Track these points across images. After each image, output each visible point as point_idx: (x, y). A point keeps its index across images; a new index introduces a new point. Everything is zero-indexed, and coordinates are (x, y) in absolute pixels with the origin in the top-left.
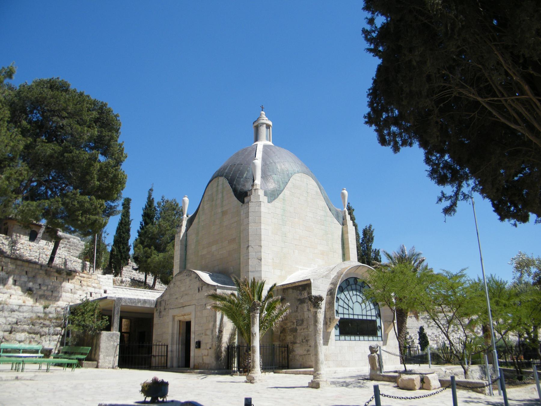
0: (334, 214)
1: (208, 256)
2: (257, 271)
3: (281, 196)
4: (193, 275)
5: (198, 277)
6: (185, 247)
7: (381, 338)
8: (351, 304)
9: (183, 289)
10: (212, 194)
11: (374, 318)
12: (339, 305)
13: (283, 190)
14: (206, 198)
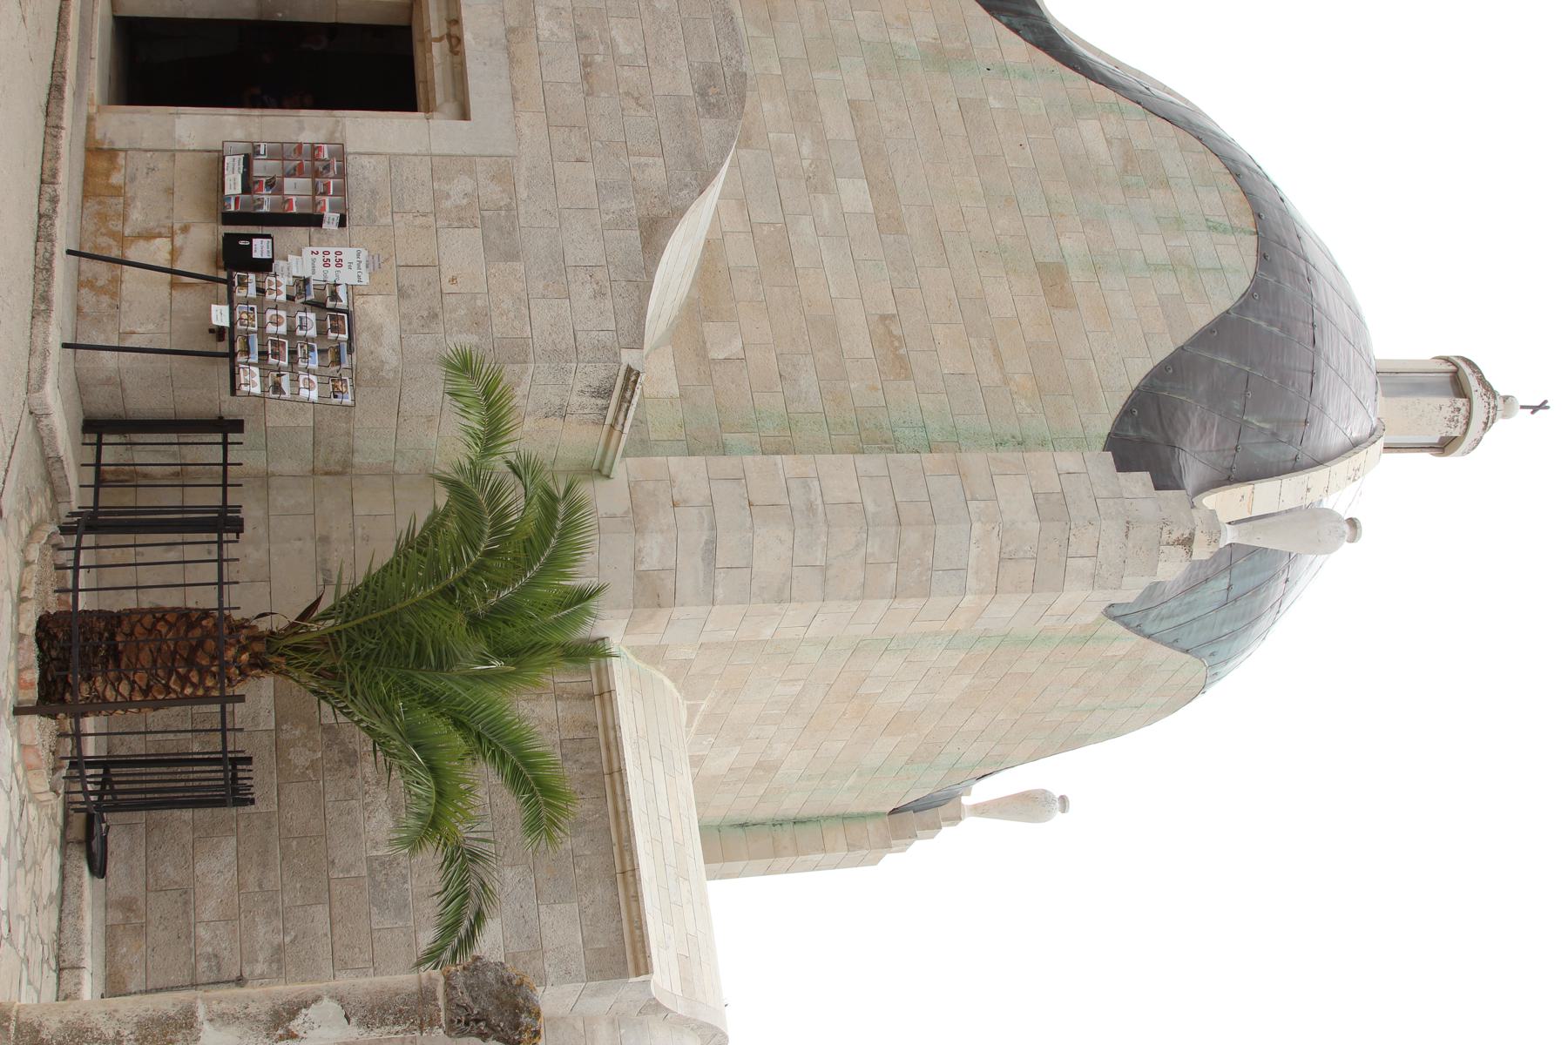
1: (805, 151)
9: (618, 33)
10: (1165, 183)
14: (1143, 131)
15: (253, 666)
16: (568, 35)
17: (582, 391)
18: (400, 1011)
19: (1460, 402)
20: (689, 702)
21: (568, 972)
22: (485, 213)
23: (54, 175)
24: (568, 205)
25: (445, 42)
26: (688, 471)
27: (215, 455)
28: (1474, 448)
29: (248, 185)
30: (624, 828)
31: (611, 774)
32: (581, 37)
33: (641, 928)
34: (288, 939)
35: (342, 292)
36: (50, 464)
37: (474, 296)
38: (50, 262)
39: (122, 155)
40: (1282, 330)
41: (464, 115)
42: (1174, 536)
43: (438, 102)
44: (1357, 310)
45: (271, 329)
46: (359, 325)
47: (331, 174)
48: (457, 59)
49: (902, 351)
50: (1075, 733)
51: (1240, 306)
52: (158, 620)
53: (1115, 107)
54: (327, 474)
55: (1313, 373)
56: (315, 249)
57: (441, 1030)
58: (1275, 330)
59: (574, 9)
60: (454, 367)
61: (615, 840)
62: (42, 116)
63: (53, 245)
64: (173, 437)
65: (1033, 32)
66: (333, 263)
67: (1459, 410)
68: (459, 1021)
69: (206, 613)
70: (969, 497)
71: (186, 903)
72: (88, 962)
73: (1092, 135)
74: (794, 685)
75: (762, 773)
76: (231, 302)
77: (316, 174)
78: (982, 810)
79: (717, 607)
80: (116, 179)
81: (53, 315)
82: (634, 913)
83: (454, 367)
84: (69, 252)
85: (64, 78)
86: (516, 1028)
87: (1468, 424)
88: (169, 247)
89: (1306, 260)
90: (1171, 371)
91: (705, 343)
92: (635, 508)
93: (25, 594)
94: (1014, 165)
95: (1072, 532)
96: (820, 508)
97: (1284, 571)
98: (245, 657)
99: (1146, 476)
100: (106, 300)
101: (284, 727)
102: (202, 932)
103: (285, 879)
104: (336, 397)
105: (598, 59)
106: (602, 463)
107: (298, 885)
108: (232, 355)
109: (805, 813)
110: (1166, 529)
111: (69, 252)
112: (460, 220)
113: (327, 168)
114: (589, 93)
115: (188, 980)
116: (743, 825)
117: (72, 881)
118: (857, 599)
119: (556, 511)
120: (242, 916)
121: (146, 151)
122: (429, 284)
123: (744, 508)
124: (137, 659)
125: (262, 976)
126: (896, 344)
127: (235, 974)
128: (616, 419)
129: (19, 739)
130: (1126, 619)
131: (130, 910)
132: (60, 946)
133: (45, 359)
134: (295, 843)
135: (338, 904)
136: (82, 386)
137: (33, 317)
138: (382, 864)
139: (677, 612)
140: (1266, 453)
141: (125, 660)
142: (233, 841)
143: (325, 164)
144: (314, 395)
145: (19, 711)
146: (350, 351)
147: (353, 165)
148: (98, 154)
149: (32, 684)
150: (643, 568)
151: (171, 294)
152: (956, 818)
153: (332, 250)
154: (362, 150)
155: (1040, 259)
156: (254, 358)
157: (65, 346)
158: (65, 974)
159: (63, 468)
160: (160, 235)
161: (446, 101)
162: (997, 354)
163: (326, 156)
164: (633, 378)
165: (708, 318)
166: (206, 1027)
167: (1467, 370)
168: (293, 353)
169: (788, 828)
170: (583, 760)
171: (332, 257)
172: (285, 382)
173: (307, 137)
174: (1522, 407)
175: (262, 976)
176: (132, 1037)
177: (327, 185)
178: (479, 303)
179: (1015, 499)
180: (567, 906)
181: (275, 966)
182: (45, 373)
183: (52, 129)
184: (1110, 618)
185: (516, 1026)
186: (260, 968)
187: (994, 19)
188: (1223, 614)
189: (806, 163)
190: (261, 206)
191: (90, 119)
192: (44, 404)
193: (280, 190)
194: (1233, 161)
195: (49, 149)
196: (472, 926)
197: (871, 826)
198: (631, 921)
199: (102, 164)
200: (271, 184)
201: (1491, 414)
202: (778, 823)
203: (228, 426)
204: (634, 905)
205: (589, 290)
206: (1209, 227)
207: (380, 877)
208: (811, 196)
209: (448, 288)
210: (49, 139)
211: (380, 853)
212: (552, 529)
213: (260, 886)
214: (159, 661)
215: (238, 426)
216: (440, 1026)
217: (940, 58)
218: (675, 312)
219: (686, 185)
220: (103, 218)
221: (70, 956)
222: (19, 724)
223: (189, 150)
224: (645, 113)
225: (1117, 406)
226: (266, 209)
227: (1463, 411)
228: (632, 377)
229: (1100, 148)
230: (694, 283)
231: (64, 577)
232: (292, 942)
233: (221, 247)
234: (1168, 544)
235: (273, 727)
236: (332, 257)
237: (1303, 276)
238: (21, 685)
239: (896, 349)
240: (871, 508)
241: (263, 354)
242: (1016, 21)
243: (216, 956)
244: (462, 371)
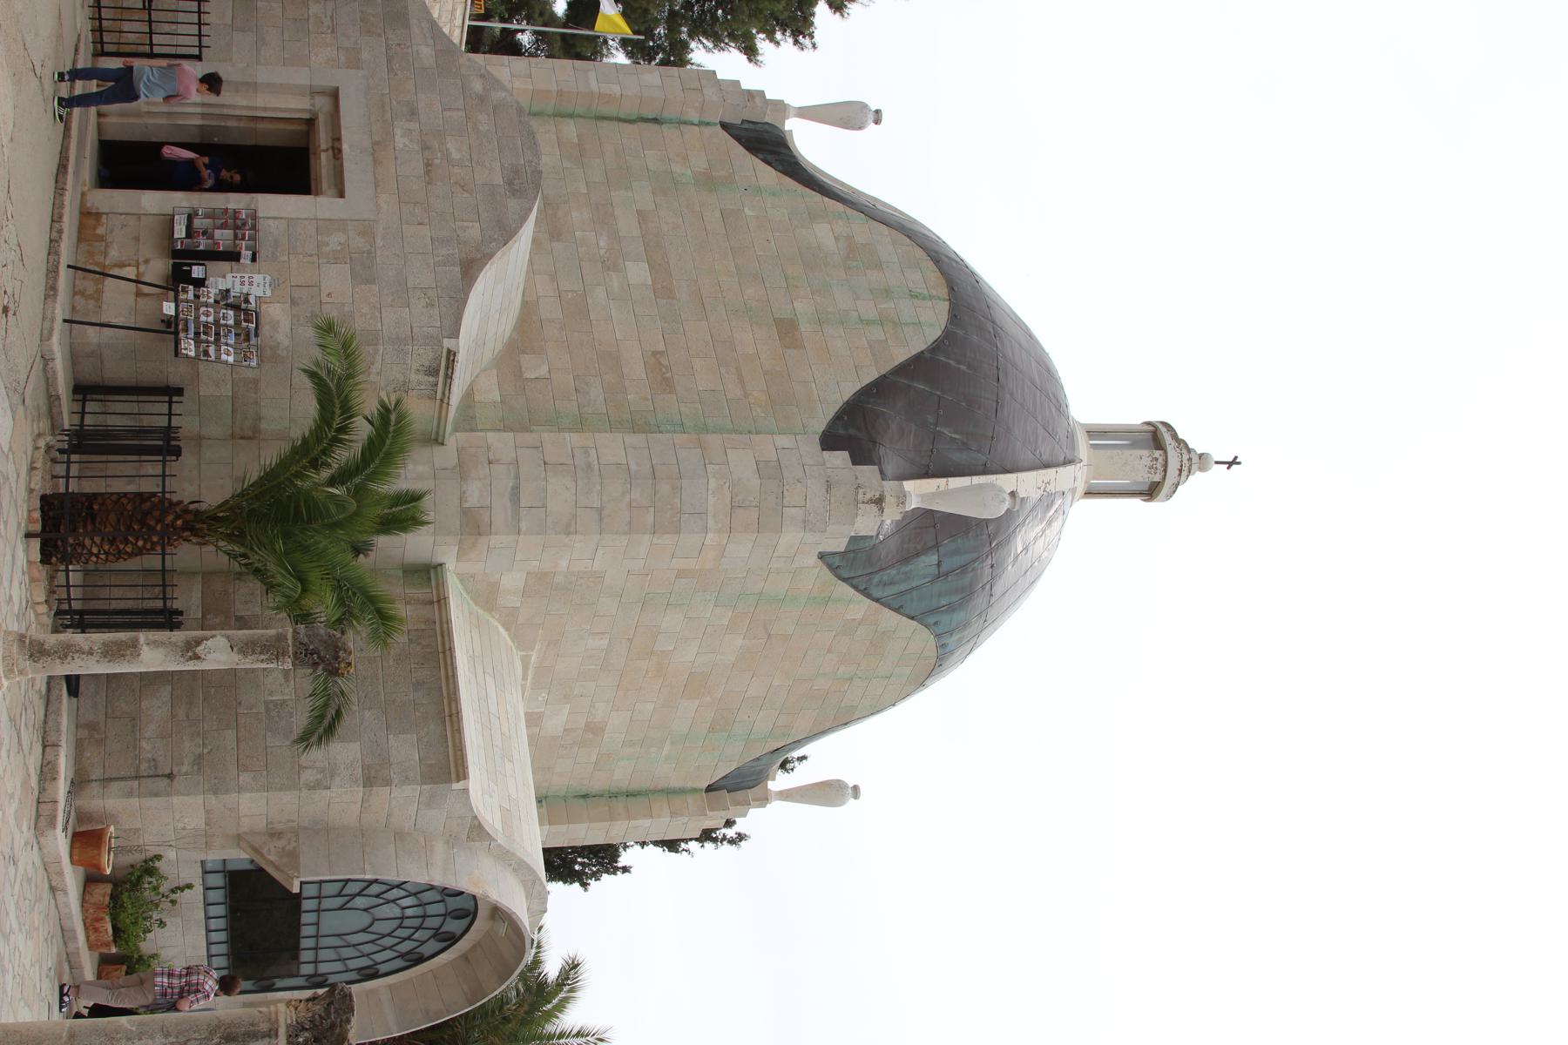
0: (755, 764)
1: (602, 244)
2: (516, 516)
3: (845, 590)
4: (513, 204)
5: (507, 234)
6: (650, 117)
8: (360, 902)
10: (879, 266)
11: (307, 969)
13: (869, 596)
14: (861, 229)
15: (184, 529)
16: (416, 147)
17: (418, 370)
18: (265, 645)
19: (1157, 453)
20: (522, 653)
21: (407, 778)
22: (353, 255)
23: (61, 217)
24: (411, 251)
25: (330, 152)
26: (501, 443)
27: (164, 408)
28: (1174, 492)
29: (190, 232)
30: (451, 686)
31: (444, 652)
32: (425, 147)
33: (461, 750)
34: (206, 751)
35: (252, 299)
36: (52, 399)
37: (343, 304)
38: (57, 268)
39: (104, 216)
40: (969, 367)
41: (341, 195)
42: (868, 497)
43: (324, 189)
44: (1046, 365)
45: (203, 318)
46: (263, 321)
47: (247, 227)
48: (337, 162)
49: (669, 375)
50: (842, 704)
51: (933, 348)
52: (122, 497)
53: (843, 215)
54: (243, 438)
55: (997, 402)
56: (235, 275)
57: (289, 660)
58: (963, 367)
59: (421, 130)
60: (321, 329)
61: (445, 694)
62: (53, 182)
63: (59, 258)
64: (134, 398)
65: (783, 165)
66: (247, 283)
67: (1157, 459)
68: (301, 653)
69: (154, 494)
70: (707, 462)
71: (134, 726)
72: (63, 743)
73: (825, 234)
74: (602, 639)
75: (591, 736)
76: (176, 301)
77: (236, 228)
78: (787, 795)
79: (522, 536)
80: (100, 231)
81: (58, 297)
82: (457, 741)
83: (321, 329)
84: (69, 266)
85: (68, 160)
86: (336, 660)
87: (1165, 471)
88: (136, 272)
89: (994, 322)
90: (875, 391)
91: (521, 368)
92: (460, 464)
93: (35, 465)
94: (762, 253)
95: (786, 487)
96: (596, 467)
97: (987, 556)
98: (179, 522)
99: (846, 454)
100: (92, 303)
101: (208, 617)
102: (144, 744)
103: (205, 712)
104: (245, 361)
105: (437, 161)
106: (437, 433)
107: (215, 717)
108: (176, 333)
109: (635, 786)
110: (861, 491)
111: (69, 266)
112: (336, 259)
113: (244, 224)
114: (430, 182)
115: (133, 774)
116: (585, 796)
117: (55, 692)
118: (625, 533)
119: (389, 420)
120: (174, 736)
121: (121, 214)
122: (313, 297)
123: (540, 466)
124: (107, 519)
125: (186, 774)
126: (664, 370)
127: (167, 771)
128: (444, 393)
129: (27, 557)
130: (855, 582)
131: (94, 729)
132: (45, 732)
133: (53, 322)
134: (213, 690)
135: (243, 730)
136: (74, 357)
137: (45, 299)
138: (276, 705)
139: (494, 540)
140: (958, 457)
141: (98, 520)
142: (169, 688)
143: (243, 222)
144: (231, 359)
145: (28, 535)
146: (256, 335)
147: (261, 225)
148: (89, 217)
149: (37, 520)
150: (467, 505)
151: (136, 300)
152: (764, 800)
153: (247, 276)
154: (269, 215)
155: (776, 316)
156: (192, 336)
157: (65, 321)
158: (48, 749)
159: (60, 405)
160: (129, 265)
161: (329, 188)
162: (741, 380)
163: (244, 217)
164: (452, 358)
165: (524, 352)
166: (145, 647)
167: (1163, 429)
168: (217, 334)
169: (622, 799)
170: (424, 643)
171: (246, 279)
172: (212, 351)
173: (231, 206)
174: (1217, 463)
175: (186, 774)
176: (99, 651)
177: (244, 235)
178: (346, 309)
179: (742, 465)
180: (409, 736)
181: (196, 768)
182: (53, 330)
183: (59, 190)
184: (839, 579)
185: (336, 658)
186: (184, 769)
187: (753, 156)
188: (938, 587)
189: (602, 252)
190: (199, 246)
191: (83, 194)
192: (51, 351)
193: (212, 237)
194: (936, 252)
195: (57, 202)
196: (333, 719)
197: (690, 798)
198: (454, 746)
199: (92, 222)
200: (205, 233)
201: (1185, 461)
202: (614, 795)
203: (172, 392)
204: (457, 735)
205: (423, 302)
206: (912, 296)
207: (274, 714)
208: (605, 273)
209: (325, 299)
210: (57, 196)
211: (274, 698)
212: (387, 432)
213: (188, 717)
214: (122, 521)
215: (179, 391)
216: (289, 657)
217: (708, 181)
218: (499, 347)
219: (495, 240)
220: (91, 254)
221: (52, 738)
222: (28, 546)
223: (150, 214)
224: (468, 195)
225: (831, 412)
226: (201, 248)
227: (1160, 460)
228: (451, 356)
229: (830, 243)
230: (515, 328)
231: (57, 485)
232: (208, 752)
233: (170, 272)
234: (863, 502)
235: (200, 616)
236: (246, 279)
237: (989, 332)
238: (30, 520)
239: (664, 373)
240: (633, 467)
241: (197, 334)
242: (769, 157)
243: (154, 760)
244: (328, 332)
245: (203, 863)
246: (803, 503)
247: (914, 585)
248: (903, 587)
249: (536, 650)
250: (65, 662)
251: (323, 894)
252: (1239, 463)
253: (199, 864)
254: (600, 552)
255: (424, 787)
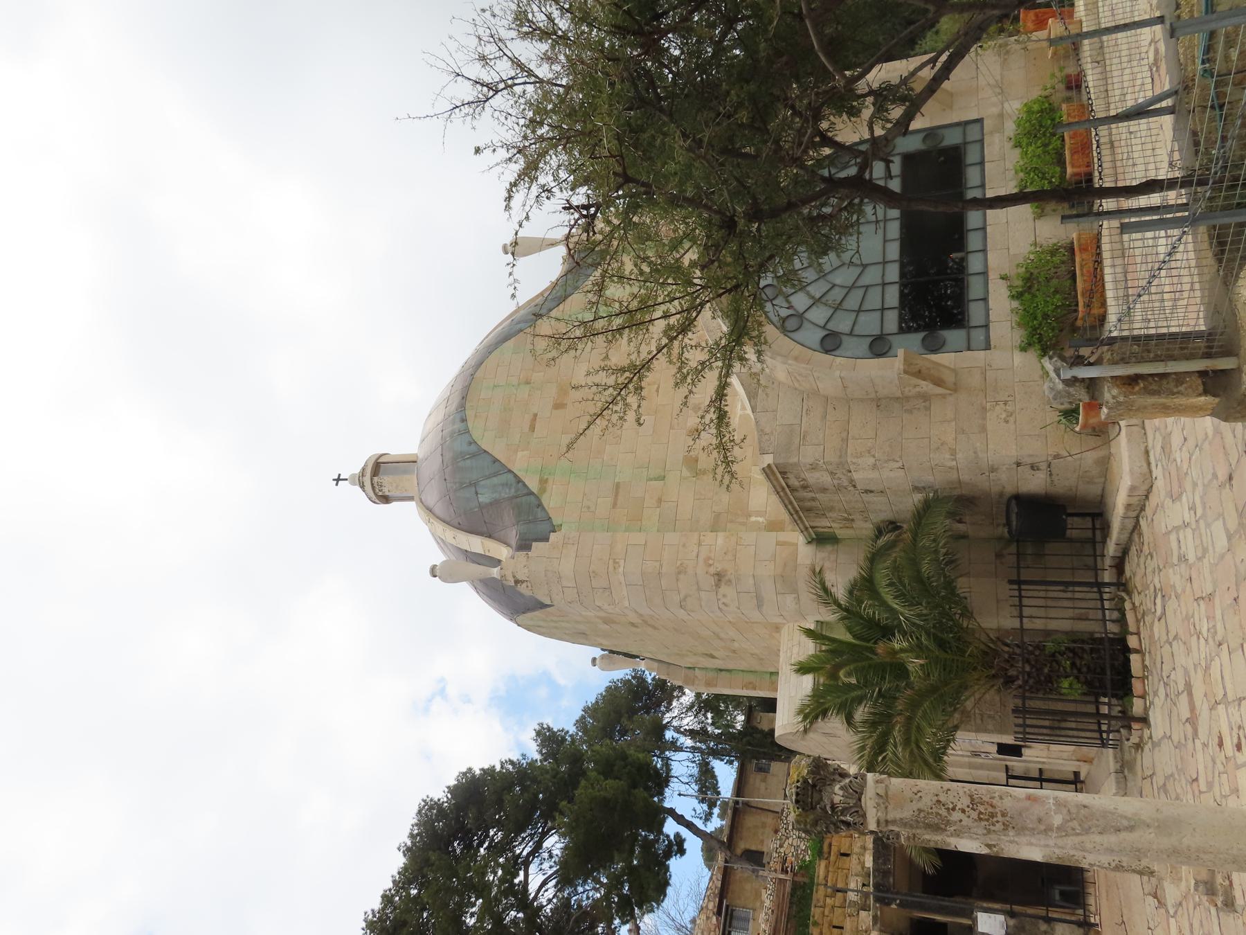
6: (723, 673)
7: (970, 127)
12: (851, 334)
13: (516, 476)
19: (380, 494)
30: (786, 502)
79: (751, 573)
87: (372, 484)
130: (525, 491)
150: (794, 595)
174: (346, 480)
227: (377, 491)
245: (988, 347)
246: (565, 589)
247: (488, 482)
248: (495, 480)
249: (738, 416)
250: (1117, 862)
251: (881, 267)
252: (334, 480)
253: (992, 343)
254: (694, 554)
255: (795, 460)
